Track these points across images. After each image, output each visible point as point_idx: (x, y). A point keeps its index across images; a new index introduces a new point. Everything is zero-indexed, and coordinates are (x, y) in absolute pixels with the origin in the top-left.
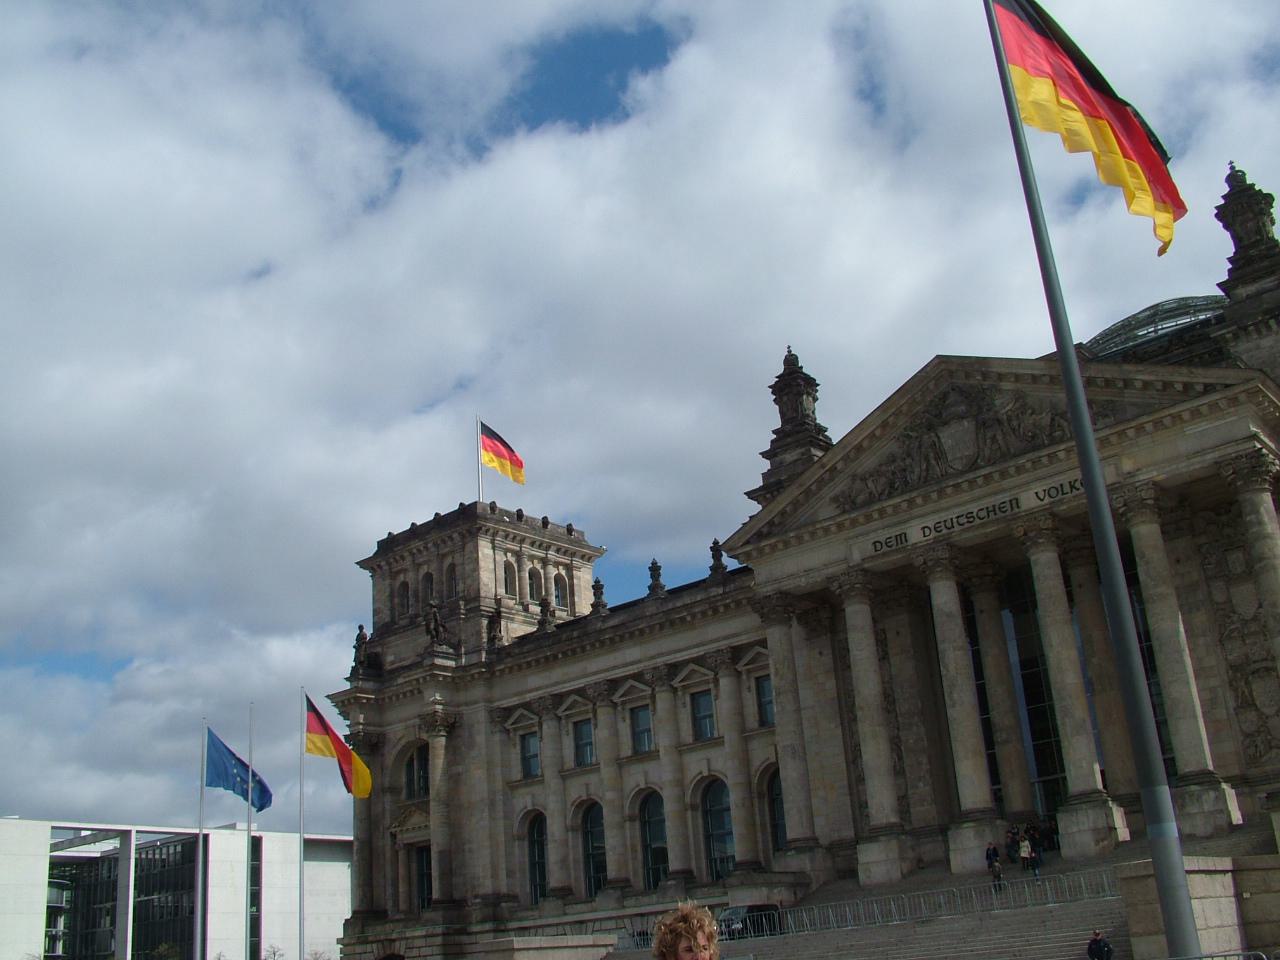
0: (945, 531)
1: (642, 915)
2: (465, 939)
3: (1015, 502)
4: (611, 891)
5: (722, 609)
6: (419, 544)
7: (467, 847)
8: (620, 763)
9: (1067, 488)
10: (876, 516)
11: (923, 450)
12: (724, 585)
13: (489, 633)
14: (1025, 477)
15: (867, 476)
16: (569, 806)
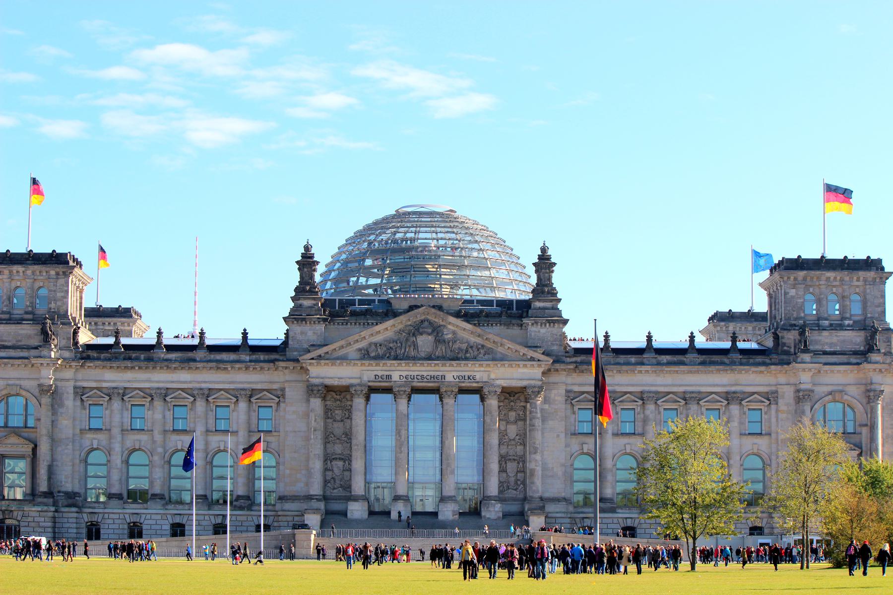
0: (410, 380)
1: (180, 514)
2: (56, 514)
3: (443, 377)
4: (159, 500)
5: (251, 369)
6: (20, 268)
7: (54, 463)
8: (165, 432)
9: (466, 378)
10: (381, 365)
11: (409, 343)
12: (250, 355)
13: (74, 339)
14: (450, 368)
15: (378, 345)
16: (124, 449)
